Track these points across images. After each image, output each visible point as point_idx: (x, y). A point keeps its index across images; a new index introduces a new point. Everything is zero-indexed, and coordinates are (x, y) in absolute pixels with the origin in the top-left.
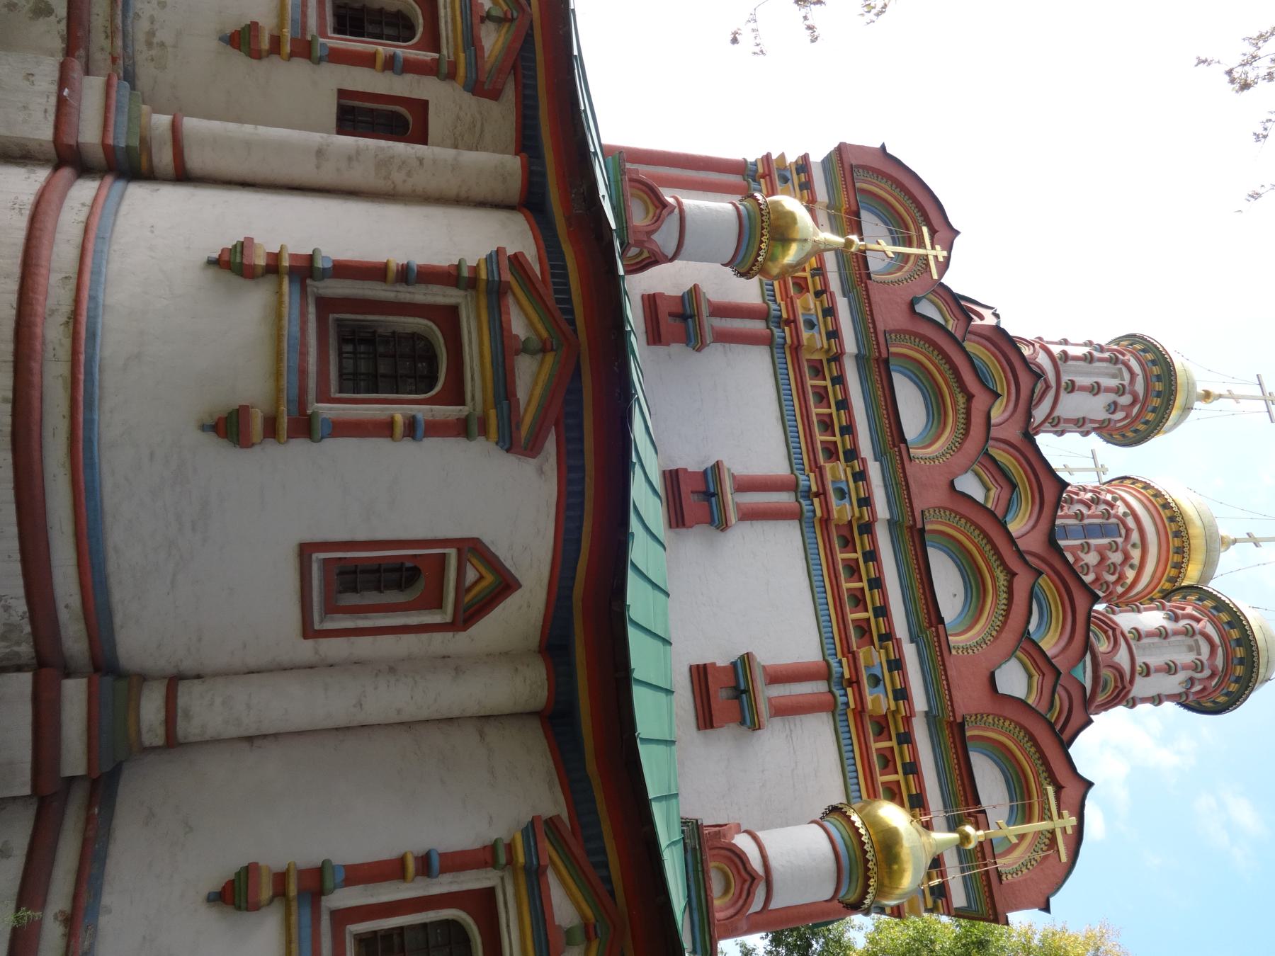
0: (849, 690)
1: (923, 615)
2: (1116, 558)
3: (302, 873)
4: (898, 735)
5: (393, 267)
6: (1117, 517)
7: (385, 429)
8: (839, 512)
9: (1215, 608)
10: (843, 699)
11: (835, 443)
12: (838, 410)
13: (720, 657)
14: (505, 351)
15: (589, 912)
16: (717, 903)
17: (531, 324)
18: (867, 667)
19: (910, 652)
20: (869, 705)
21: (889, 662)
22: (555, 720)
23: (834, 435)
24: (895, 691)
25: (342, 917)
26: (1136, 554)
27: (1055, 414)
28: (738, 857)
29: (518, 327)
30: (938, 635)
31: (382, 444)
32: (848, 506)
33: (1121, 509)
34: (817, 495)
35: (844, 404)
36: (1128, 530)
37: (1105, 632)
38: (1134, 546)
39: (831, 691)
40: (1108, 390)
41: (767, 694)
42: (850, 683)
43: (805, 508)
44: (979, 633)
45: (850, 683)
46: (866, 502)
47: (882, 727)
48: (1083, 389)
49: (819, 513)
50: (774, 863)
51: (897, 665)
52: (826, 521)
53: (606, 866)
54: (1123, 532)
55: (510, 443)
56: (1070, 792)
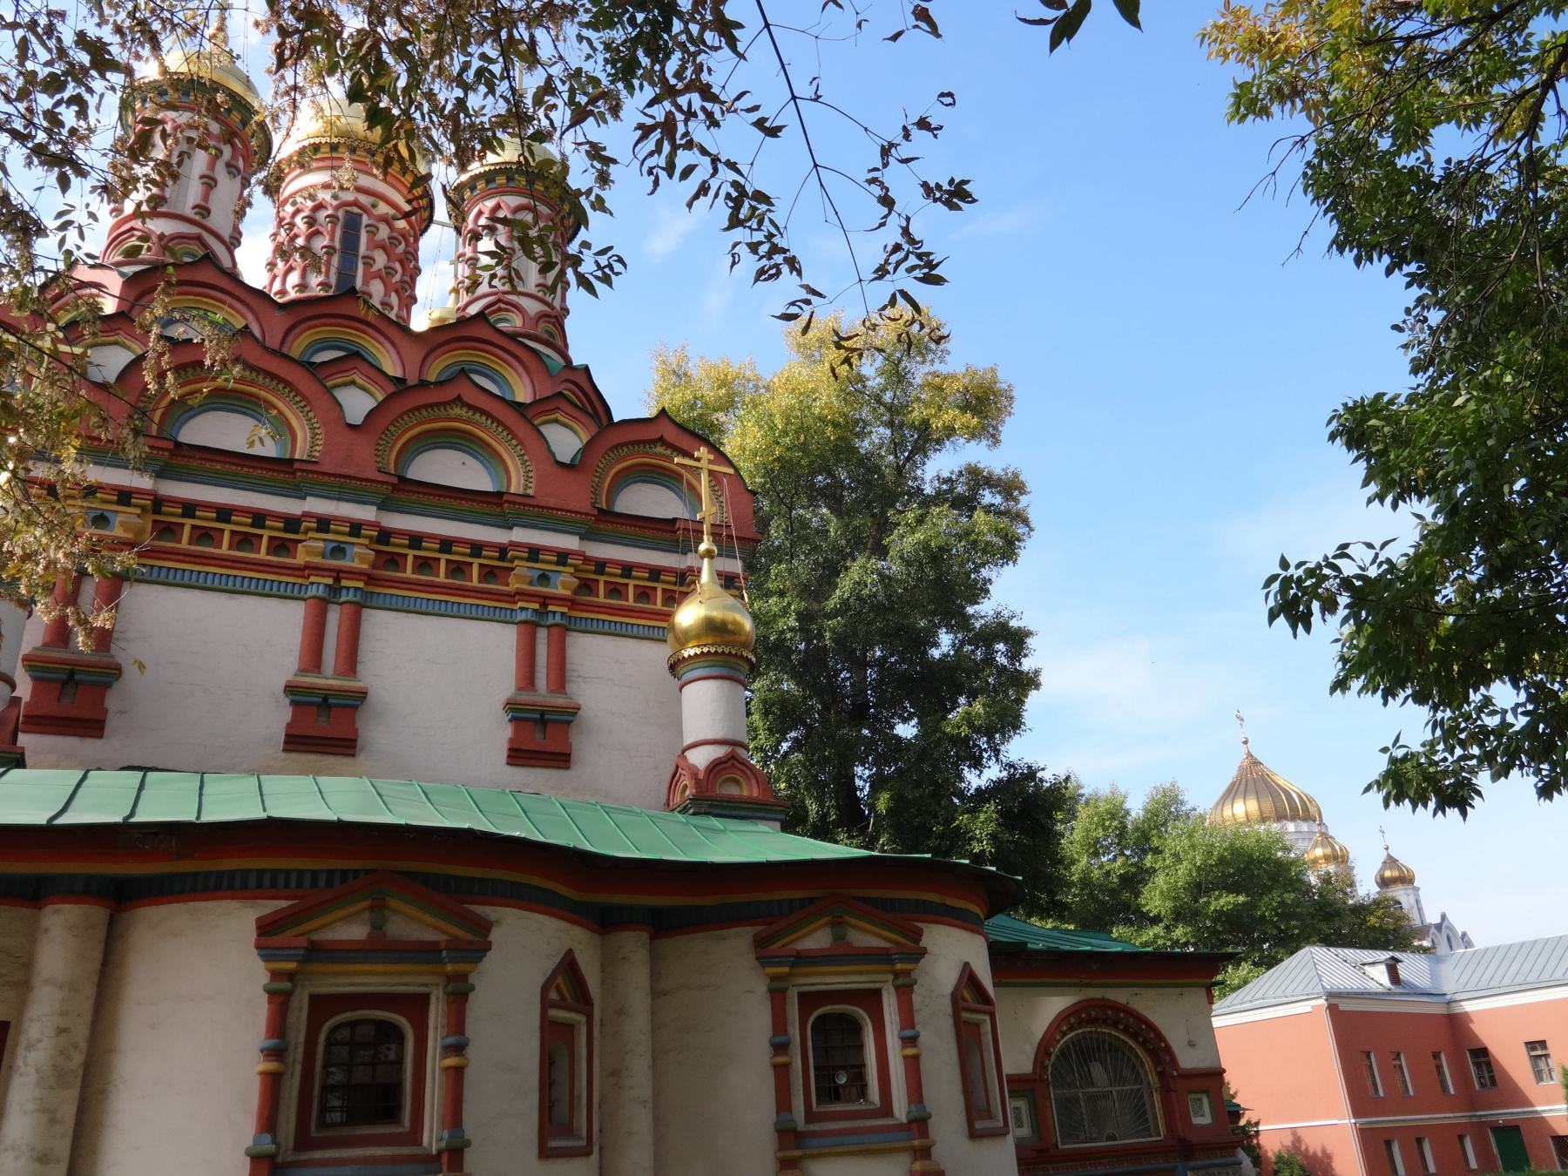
0: (550, 608)
1: (487, 509)
2: (384, 232)
3: (781, 1147)
4: (595, 572)
5: (262, 1067)
6: (337, 208)
7: (456, 1076)
8: (362, 561)
9: (488, 182)
10: (558, 617)
11: (271, 538)
12: (229, 521)
13: (502, 733)
14: (379, 949)
15: (825, 920)
16: (745, 793)
17: (348, 919)
18: (531, 583)
19: (520, 535)
20: (568, 593)
21: (528, 560)
22: (662, 925)
23: (261, 536)
24: (558, 563)
25: (810, 1117)
26: (383, 209)
27: (227, 239)
28: (715, 767)
29: (355, 932)
30: (514, 503)
31: (469, 1075)
32: (356, 549)
33: (325, 196)
34: (337, 579)
35: (224, 513)
36: (355, 203)
37: (500, 309)
38: (374, 206)
39: (549, 627)
40: (212, 166)
41: (542, 692)
42: (544, 605)
43: (351, 597)
44: (513, 459)
45: (544, 605)
46: (356, 528)
47: (587, 586)
48: (206, 198)
49: (360, 584)
50: (719, 735)
51: (534, 553)
52: (370, 579)
53: (791, 901)
54: (356, 210)
55: (477, 949)
56: (670, 434)
